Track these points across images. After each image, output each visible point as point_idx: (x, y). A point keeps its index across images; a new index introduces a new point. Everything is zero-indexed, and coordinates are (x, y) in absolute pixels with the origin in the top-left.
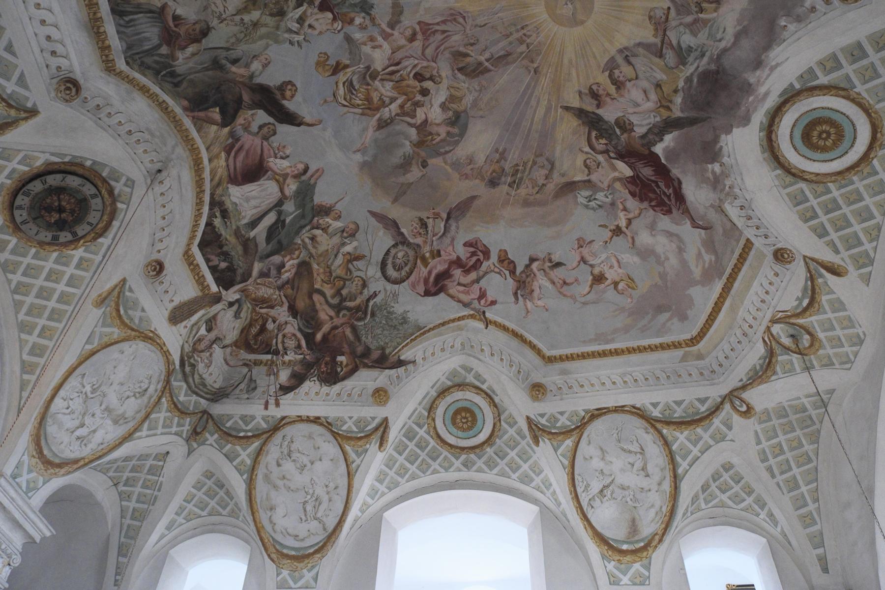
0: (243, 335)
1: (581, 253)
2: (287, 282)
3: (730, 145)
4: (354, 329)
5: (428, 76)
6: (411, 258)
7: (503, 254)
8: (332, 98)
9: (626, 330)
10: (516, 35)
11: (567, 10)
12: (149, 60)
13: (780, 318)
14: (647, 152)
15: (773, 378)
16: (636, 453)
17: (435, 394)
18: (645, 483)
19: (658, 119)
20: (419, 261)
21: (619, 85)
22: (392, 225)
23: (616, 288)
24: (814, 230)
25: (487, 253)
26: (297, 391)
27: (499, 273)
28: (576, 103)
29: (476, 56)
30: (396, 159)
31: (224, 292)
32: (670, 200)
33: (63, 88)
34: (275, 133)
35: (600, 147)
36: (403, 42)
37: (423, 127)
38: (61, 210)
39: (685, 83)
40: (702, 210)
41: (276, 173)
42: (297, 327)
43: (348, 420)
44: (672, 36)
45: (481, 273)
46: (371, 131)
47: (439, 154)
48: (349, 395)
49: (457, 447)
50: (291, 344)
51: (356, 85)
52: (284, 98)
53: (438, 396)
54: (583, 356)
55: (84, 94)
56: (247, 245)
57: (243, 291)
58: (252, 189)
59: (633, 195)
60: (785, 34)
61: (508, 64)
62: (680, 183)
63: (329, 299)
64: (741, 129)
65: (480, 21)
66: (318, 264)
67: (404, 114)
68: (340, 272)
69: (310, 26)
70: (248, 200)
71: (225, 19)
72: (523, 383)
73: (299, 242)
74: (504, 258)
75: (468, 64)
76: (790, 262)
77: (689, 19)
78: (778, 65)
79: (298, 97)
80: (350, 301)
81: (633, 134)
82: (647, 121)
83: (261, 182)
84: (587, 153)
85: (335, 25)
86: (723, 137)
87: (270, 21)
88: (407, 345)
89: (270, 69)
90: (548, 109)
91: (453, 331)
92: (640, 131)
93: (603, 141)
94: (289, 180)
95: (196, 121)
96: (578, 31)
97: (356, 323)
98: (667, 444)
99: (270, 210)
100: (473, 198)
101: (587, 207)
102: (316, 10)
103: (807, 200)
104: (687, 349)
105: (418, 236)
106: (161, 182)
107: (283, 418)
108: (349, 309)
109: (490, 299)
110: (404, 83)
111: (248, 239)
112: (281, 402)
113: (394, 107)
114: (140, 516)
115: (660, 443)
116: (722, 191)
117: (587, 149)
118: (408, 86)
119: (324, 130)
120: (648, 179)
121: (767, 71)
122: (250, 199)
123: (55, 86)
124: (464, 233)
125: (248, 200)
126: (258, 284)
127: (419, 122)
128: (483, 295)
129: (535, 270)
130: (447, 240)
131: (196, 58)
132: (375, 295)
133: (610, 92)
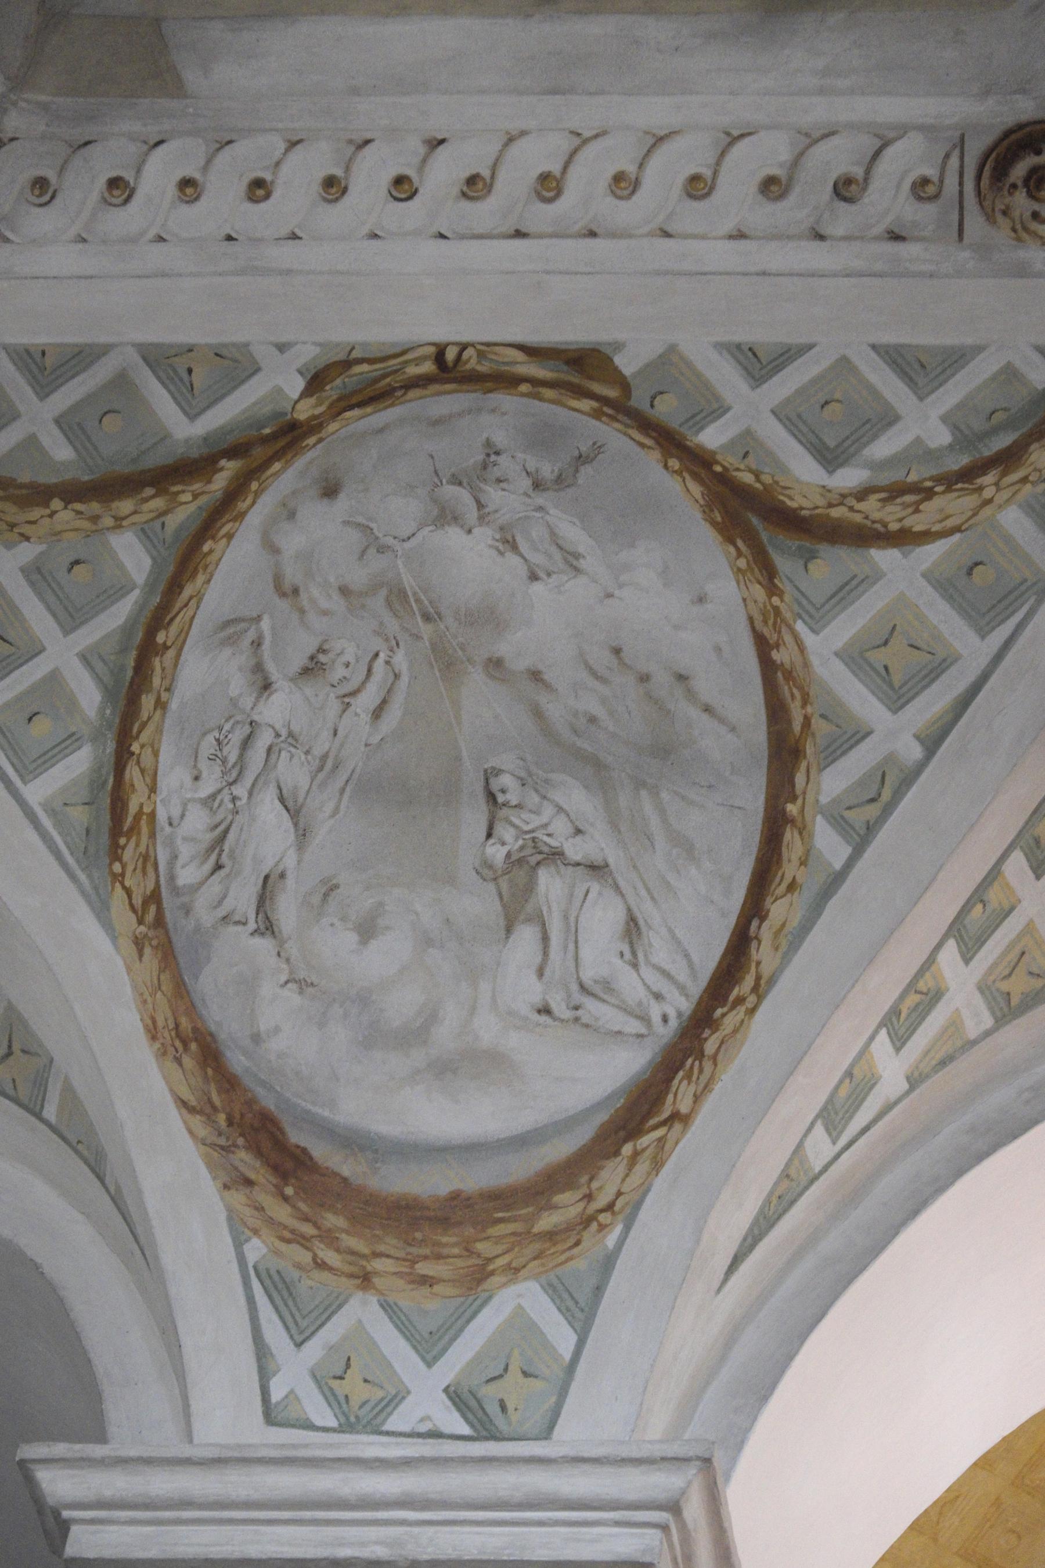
33: (1021, 201)
123: (1002, 235)
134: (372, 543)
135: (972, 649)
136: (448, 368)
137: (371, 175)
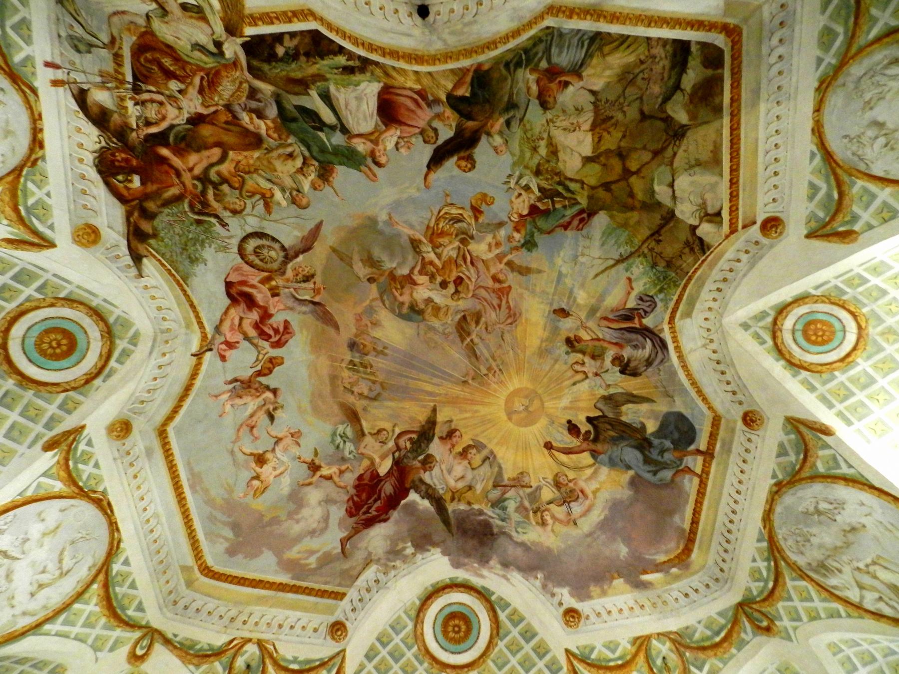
0: (164, 47)
1: (286, 437)
2: (235, 117)
3: (433, 557)
4: (178, 199)
5: (460, 289)
6: (269, 266)
8: (449, 201)
9: (210, 502)
10: (494, 364)
11: (518, 405)
12: (541, 48)
13: (266, 649)
14: (407, 486)
15: (191, 667)
17: (94, 304)
19: (441, 492)
20: (266, 274)
21: (464, 454)
22: (306, 247)
23: (254, 478)
24: (372, 648)
25: (278, 344)
26: (81, 115)
27: (257, 360)
28: (441, 418)
29: (476, 331)
30: (377, 253)
31: (240, 41)
32: (364, 513)
34: (425, 142)
35: (402, 442)
36: (493, 271)
37: (409, 280)
40: (363, 545)
41: (381, 133)
42: (176, 122)
43: (45, 190)
44: (511, 493)
45: (256, 341)
46: (411, 232)
47: (381, 295)
48: (84, 192)
50: (152, 112)
51: (455, 226)
52: (459, 159)
53: (90, 308)
54: (172, 468)
56: (303, 85)
57: (235, 64)
58: (371, 104)
59: (360, 478)
60: (532, 580)
61: (469, 357)
62: (385, 520)
63: (216, 168)
64: (448, 562)
65: (507, 337)
66: (258, 158)
67: (424, 265)
68: (250, 184)
69: (520, 195)
70: (359, 99)
71: (548, 124)
72: (129, 410)
73: (289, 141)
74: (274, 362)
76: (333, 638)
77: (527, 504)
78: (508, 579)
79: (456, 171)
80: (215, 194)
81: (422, 471)
83: (375, 117)
84: (393, 431)
85: (516, 216)
86: (439, 550)
87: (535, 161)
88: (163, 265)
89: (492, 151)
90: (431, 394)
91: (185, 318)
92: (426, 477)
93: (408, 445)
95: (464, 71)
97: (187, 201)
98: (78, 596)
100: (337, 327)
101: (334, 434)
102: (532, 202)
103: (397, 634)
104: (196, 568)
105: (295, 272)
106: (410, 15)
107: (34, 91)
108: (204, 193)
109: (228, 354)
110: (453, 267)
111: (307, 87)
112: (61, 89)
113: (432, 256)
116: (389, 560)
117: (397, 431)
118: (451, 271)
119: (418, 189)
120: (380, 491)
121: (501, 573)
122: (359, 102)
124: (299, 320)
125: (359, 99)
126: (241, 83)
127: (415, 277)
128: (230, 345)
129: (264, 396)
130: (290, 303)
131: (525, 90)
132: (224, 225)
133: (456, 447)
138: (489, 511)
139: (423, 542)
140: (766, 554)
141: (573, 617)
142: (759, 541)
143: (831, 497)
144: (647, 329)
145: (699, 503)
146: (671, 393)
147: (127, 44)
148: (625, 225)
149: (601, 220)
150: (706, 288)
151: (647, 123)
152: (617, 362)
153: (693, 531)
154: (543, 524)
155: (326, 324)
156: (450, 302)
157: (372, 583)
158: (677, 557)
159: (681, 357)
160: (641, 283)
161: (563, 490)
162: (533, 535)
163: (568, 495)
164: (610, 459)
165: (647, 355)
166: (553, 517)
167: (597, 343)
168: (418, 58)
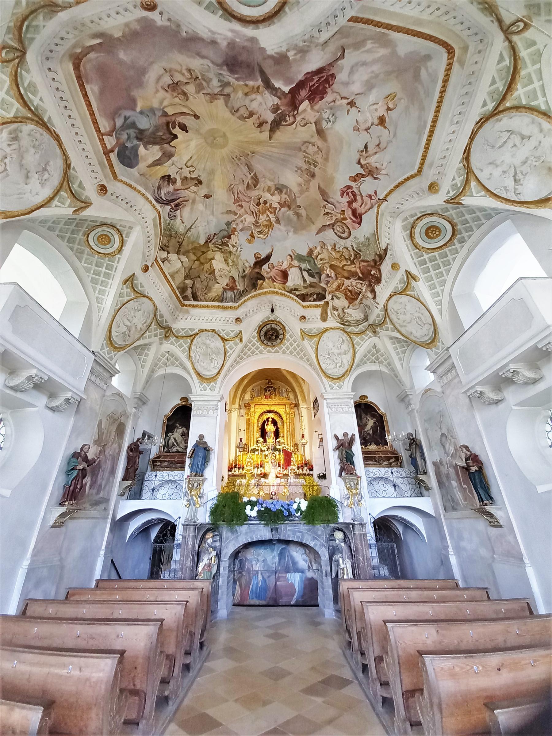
2: (336, 275)
4: (363, 261)
6: (341, 224)
7: (351, 178)
10: (237, 161)
11: (220, 140)
16: (509, 138)
18: (533, 142)
19: (266, 92)
21: (251, 114)
25: (349, 187)
27: (361, 184)
28: (267, 134)
29: (248, 180)
30: (295, 218)
31: (326, 300)
32: (323, 77)
35: (292, 119)
36: (243, 210)
37: (282, 205)
38: (272, 335)
39: (240, 81)
44: (217, 90)
47: (295, 199)
49: (448, 242)
50: (359, 286)
55: (241, 318)
56: (311, 285)
62: (308, 73)
67: (275, 212)
70: (294, 280)
75: (252, 183)
78: (210, 31)
82: (269, 97)
87: (232, 257)
90: (272, 146)
92: (276, 101)
93: (287, 118)
94: (292, 263)
95: (260, 289)
96: (228, 134)
99: (302, 273)
100: (319, 187)
107: (384, 306)
108: (354, 259)
113: (271, 216)
114: (389, 364)
115: (514, 113)
116: (308, 46)
117: (294, 125)
120: (309, 92)
122: (295, 279)
128: (370, 197)
130: (337, 205)
132: (352, 246)
134: (202, 340)
135: (235, 347)
136: (206, 330)
137: (201, 319)
138: (231, 80)
139: (281, 60)
140: (40, 112)
141: (147, 5)
142: (50, 117)
143: (48, 183)
144: (167, 204)
145: (92, 114)
146: (142, 177)
147: (357, 302)
148: (193, 243)
149: (202, 241)
150: (153, 234)
151: (197, 275)
152: (174, 180)
153: (82, 87)
154: (189, 70)
155: (324, 190)
156: (262, 194)
157: (324, 29)
158: (81, 60)
159: (147, 199)
160: (178, 224)
161: (180, 91)
162: (197, 64)
163: (174, 87)
164: (155, 114)
165: (162, 191)
166: (183, 74)
167: (187, 187)
168: (274, 292)
